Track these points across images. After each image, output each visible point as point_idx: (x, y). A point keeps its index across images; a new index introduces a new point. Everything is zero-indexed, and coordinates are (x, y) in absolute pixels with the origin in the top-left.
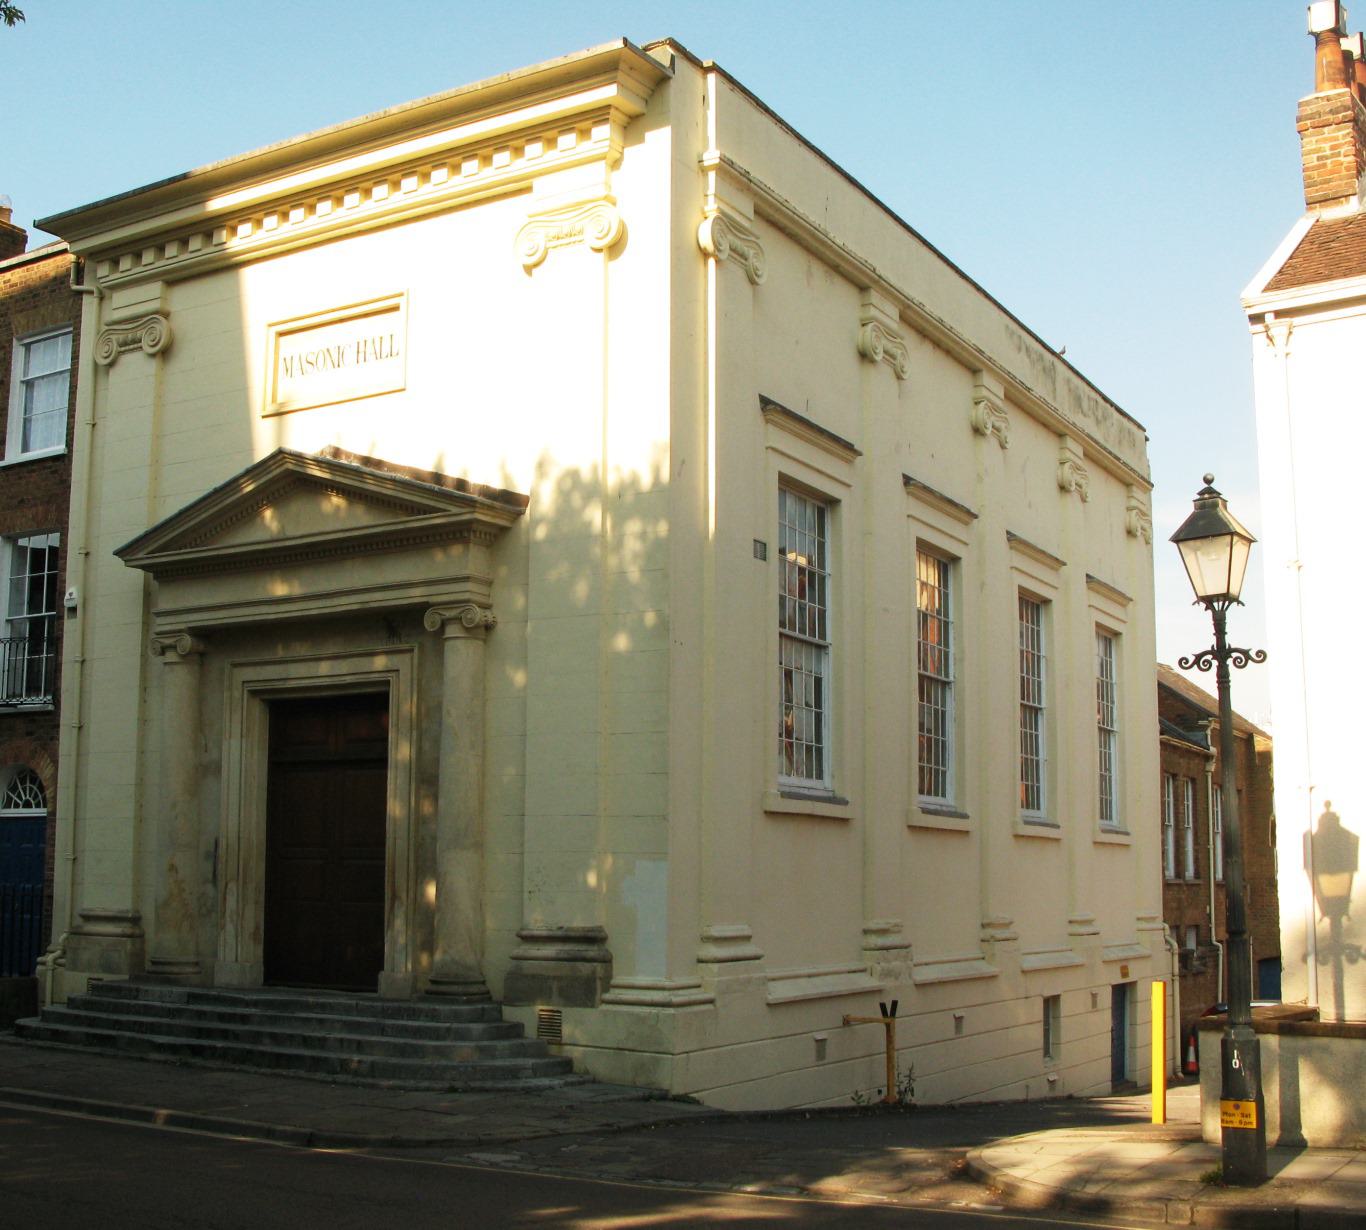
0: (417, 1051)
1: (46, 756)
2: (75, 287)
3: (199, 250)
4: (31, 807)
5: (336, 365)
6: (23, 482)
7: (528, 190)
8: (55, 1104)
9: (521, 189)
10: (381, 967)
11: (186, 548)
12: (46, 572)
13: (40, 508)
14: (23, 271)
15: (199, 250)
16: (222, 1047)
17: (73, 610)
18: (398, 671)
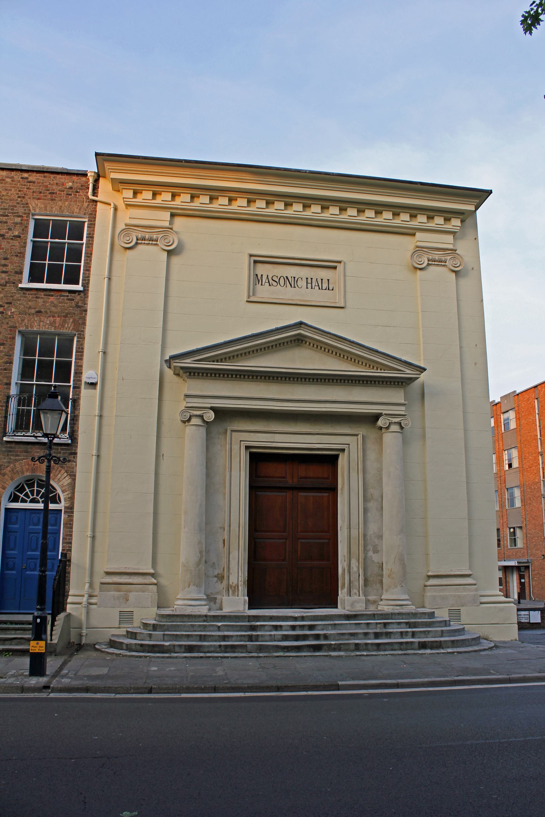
0: (257, 638)
1: (63, 471)
2: (91, 197)
3: (391, 220)
4: (40, 503)
5: (293, 286)
6: (40, 300)
7: (414, 235)
8: (397, 686)
9: (411, 233)
10: (338, 595)
11: (217, 362)
12: (37, 357)
13: (58, 319)
14: (40, 176)
15: (391, 220)
16: (335, 644)
17: (93, 385)
18: (349, 444)
